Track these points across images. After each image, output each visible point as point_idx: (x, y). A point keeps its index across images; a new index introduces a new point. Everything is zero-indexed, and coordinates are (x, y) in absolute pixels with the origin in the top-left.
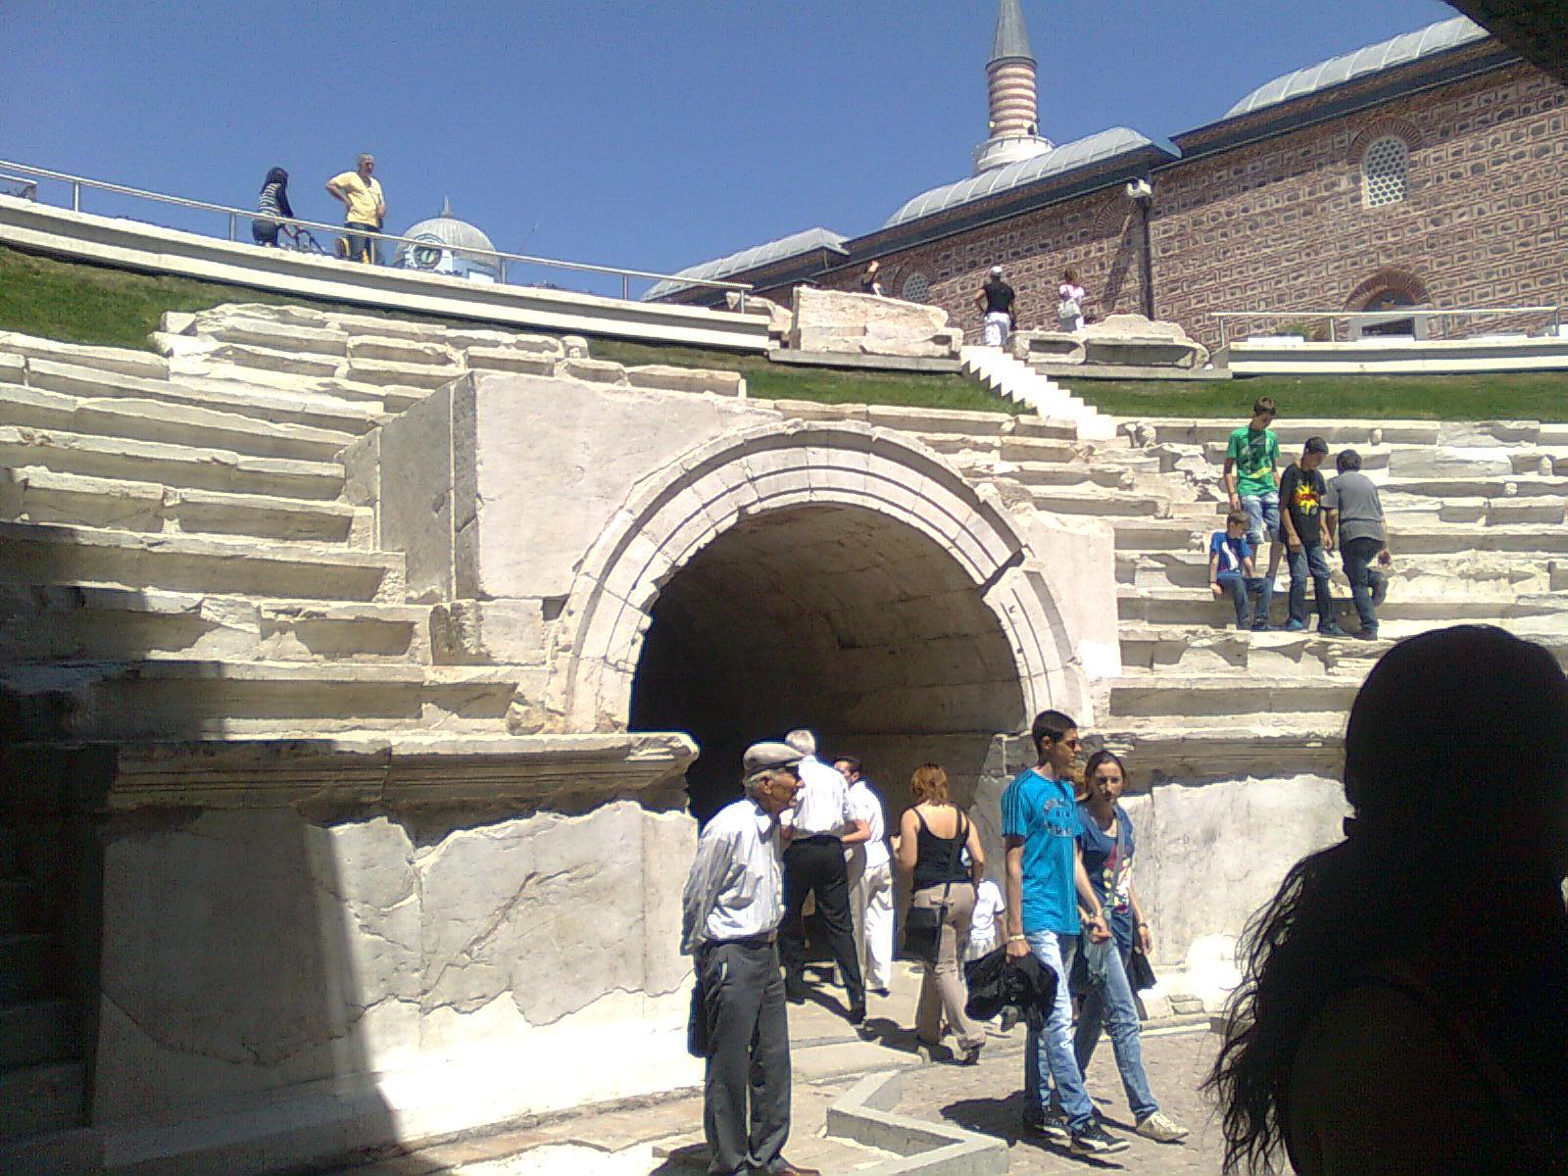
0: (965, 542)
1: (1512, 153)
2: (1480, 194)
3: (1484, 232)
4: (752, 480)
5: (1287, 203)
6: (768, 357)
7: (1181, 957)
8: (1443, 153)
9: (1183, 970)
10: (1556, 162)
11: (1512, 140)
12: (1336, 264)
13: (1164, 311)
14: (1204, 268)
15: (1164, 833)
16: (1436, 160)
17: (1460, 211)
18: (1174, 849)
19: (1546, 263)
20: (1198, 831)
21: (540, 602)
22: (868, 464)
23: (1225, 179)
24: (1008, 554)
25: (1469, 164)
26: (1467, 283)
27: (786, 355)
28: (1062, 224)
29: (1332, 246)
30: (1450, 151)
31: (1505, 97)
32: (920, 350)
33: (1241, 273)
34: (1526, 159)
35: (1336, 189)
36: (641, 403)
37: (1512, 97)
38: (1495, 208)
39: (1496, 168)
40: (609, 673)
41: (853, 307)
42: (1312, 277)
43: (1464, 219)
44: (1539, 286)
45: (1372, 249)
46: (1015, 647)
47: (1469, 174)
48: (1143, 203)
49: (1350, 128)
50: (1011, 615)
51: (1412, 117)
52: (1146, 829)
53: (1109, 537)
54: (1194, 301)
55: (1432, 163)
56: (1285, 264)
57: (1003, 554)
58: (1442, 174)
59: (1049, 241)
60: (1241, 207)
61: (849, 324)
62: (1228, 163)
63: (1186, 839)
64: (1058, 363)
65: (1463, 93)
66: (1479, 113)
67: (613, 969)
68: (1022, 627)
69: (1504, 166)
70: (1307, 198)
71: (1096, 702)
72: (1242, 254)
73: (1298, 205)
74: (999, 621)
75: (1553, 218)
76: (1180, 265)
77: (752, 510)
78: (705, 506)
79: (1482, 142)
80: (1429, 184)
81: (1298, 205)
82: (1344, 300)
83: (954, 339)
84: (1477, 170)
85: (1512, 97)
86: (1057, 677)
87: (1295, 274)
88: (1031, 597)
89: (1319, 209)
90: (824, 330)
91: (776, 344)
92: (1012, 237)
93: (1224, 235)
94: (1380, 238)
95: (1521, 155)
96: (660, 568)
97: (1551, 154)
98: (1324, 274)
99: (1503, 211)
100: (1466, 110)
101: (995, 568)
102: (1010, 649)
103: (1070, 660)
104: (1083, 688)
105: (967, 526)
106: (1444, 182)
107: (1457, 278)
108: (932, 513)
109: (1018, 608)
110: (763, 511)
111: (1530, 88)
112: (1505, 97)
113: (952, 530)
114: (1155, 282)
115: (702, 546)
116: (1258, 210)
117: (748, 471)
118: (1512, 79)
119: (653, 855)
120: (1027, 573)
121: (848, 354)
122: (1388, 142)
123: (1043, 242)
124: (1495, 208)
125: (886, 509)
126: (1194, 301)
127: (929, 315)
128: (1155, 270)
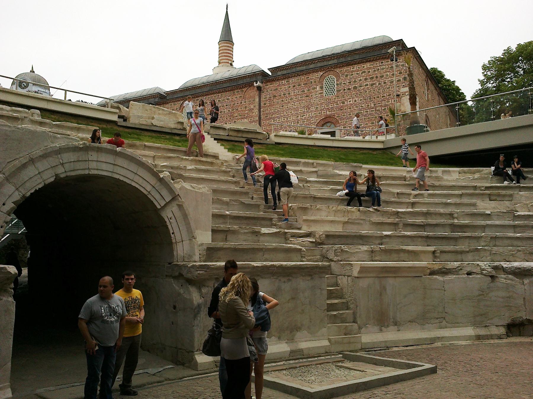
0: (154, 193)
1: (365, 84)
2: (356, 95)
3: (356, 107)
4: (62, 164)
5: (301, 93)
6: (117, 123)
8: (346, 82)
10: (376, 88)
11: (365, 80)
12: (314, 113)
13: (264, 123)
14: (276, 111)
16: (345, 83)
17: (350, 100)
19: (372, 118)
22: (115, 161)
23: (284, 83)
24: (170, 198)
25: (353, 86)
26: (350, 122)
27: (124, 124)
28: (234, 93)
29: (314, 107)
30: (348, 82)
31: (363, 67)
32: (173, 126)
33: (287, 113)
34: (369, 86)
35: (316, 90)
36: (13, 131)
37: (365, 67)
38: (359, 101)
39: (360, 88)
41: (150, 110)
42: (308, 116)
43: (351, 102)
44: (370, 124)
45: (325, 109)
46: (171, 232)
47: (353, 89)
48: (259, 88)
49: (321, 71)
50: (170, 220)
51: (338, 70)
53: (210, 193)
54: (272, 121)
55: (343, 85)
56: (299, 111)
57: (168, 198)
58: (345, 88)
59: (230, 98)
60: (288, 93)
61: (149, 115)
62: (285, 79)
65: (352, 65)
66: (356, 71)
68: (174, 224)
69: (363, 87)
70: (307, 92)
71: (201, 252)
72: (288, 107)
73: (305, 94)
74: (166, 222)
75: (375, 104)
76: (269, 109)
77: (62, 176)
79: (357, 80)
80: (341, 91)
81: (305, 94)
82: (316, 124)
84: (355, 88)
85: (365, 67)
86: (186, 243)
87: (302, 115)
88: (178, 213)
89: (310, 95)
90: (139, 117)
91: (122, 120)
92: (218, 96)
93: (282, 101)
94: (327, 106)
95: (367, 85)
96: (17, 197)
97: (375, 86)
98: (311, 116)
99: (362, 101)
100: (353, 70)
101: (166, 203)
102: (170, 232)
103: (192, 237)
104: (196, 247)
105: (155, 187)
106: (346, 91)
107: (348, 120)
108: (141, 181)
109: (173, 217)
110: (67, 176)
111: (370, 65)
112: (363, 67)
113: (149, 188)
114: (262, 113)
115: (37, 189)
116: (293, 94)
117: (61, 161)
118: (366, 62)
120: (178, 205)
121: (147, 125)
122: (331, 77)
123: (228, 98)
124: (359, 101)
125: (122, 178)
126: (272, 121)
127: (178, 115)
128: (262, 110)
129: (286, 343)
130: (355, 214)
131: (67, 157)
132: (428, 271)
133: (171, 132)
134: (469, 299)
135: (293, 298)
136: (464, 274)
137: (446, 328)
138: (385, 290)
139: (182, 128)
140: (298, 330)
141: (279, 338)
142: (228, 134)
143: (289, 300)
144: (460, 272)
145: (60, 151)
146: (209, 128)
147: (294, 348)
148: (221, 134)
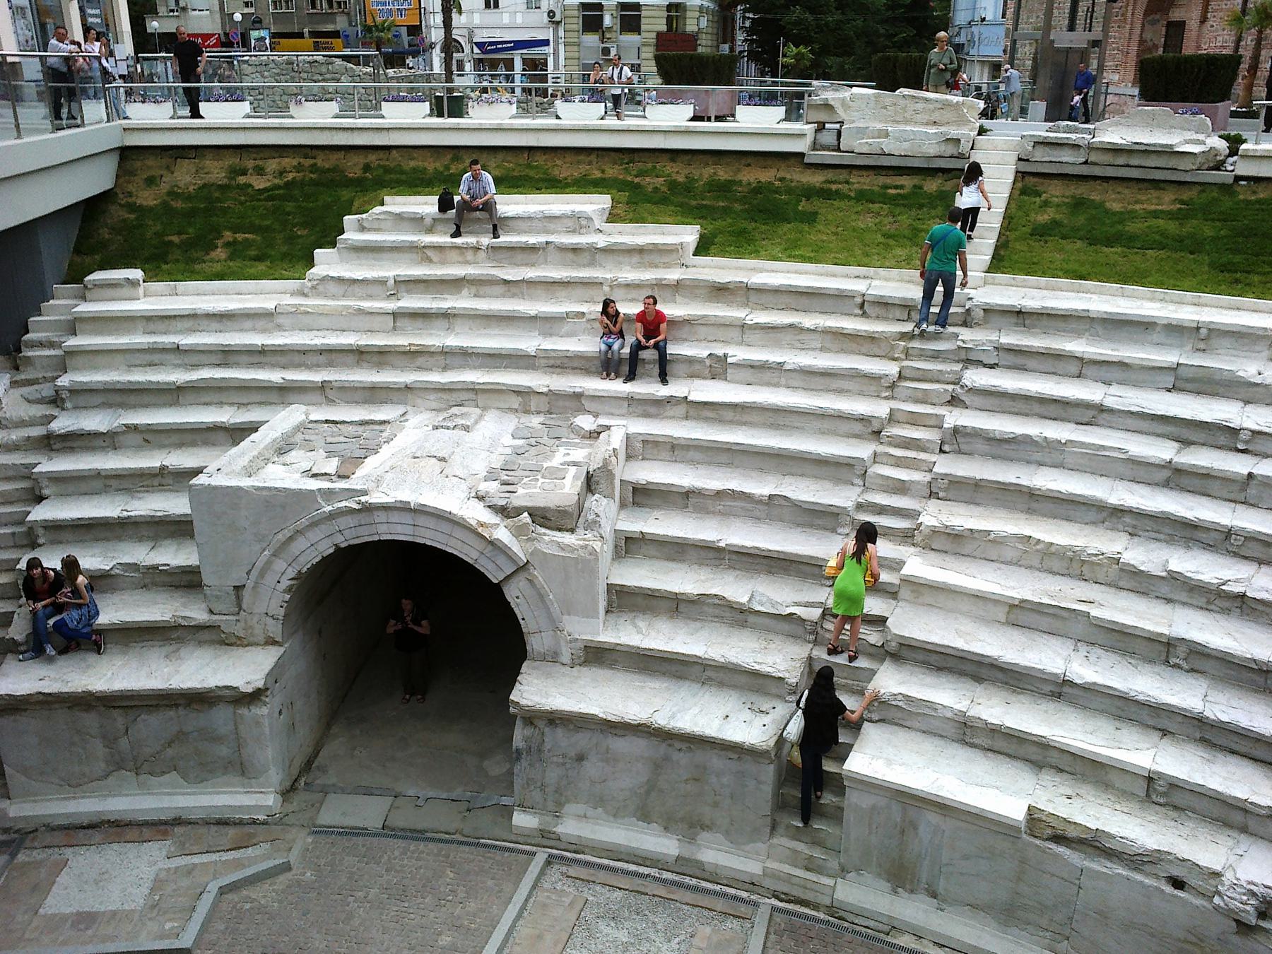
9: (557, 816)
20: (573, 754)
32: (932, 150)
40: (269, 620)
46: (520, 617)
52: (538, 746)
63: (564, 756)
64: (1059, 162)
67: (226, 768)
77: (343, 545)
83: (962, 142)
88: (528, 591)
96: (291, 573)
103: (557, 629)
119: (241, 727)
129: (679, 840)
130: (1105, 569)
131: (344, 522)
132: (1049, 831)
133: (926, 166)
134: (1152, 935)
136: (1157, 877)
138: (915, 828)
139: (956, 154)
140: (706, 829)
142: (1084, 160)
144: (1147, 868)
145: (332, 516)
146: (1030, 148)
147: (686, 855)
148: (1065, 159)
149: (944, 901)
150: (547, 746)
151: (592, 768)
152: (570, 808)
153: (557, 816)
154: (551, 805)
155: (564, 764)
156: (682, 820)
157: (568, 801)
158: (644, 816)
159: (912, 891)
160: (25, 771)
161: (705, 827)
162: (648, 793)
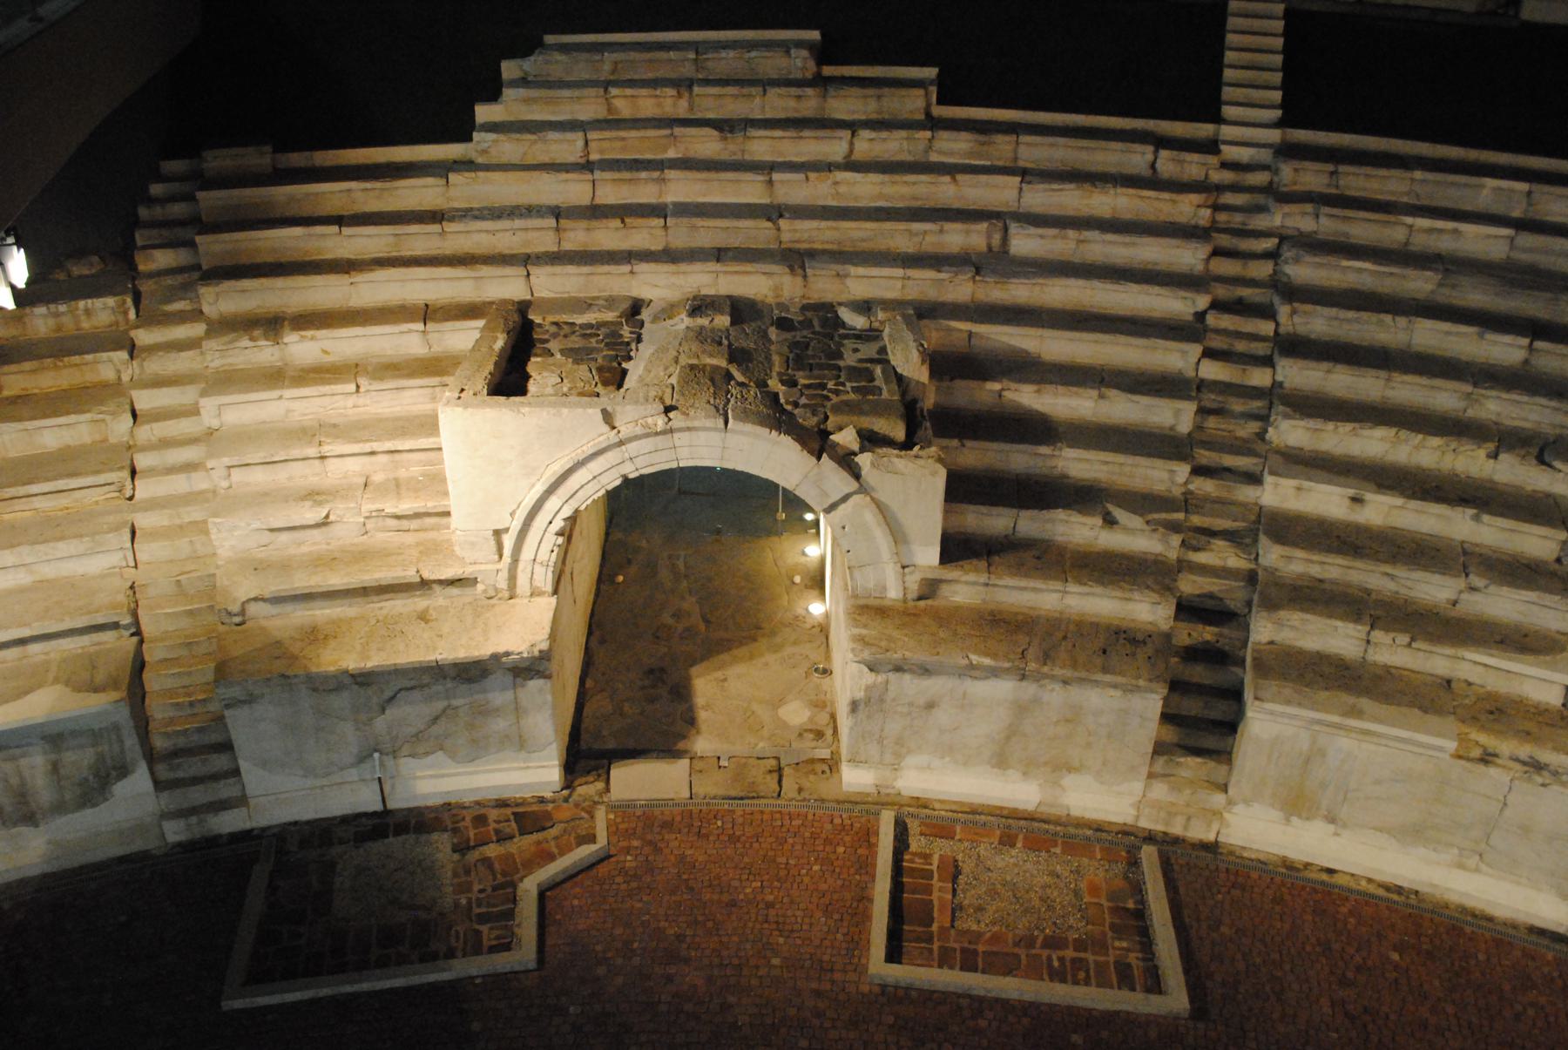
7: (896, 762)
9: (896, 769)
15: (894, 700)
18: (899, 709)
21: (492, 532)
77: (631, 476)
78: (595, 477)
129: (1040, 785)
135: (1067, 721)
137: (1477, 870)
141: (1025, 774)
143: (1058, 721)
149: (1345, 826)
150: (891, 694)
151: (942, 716)
152: (910, 761)
153: (896, 769)
154: (888, 758)
155: (910, 713)
156: (1046, 764)
157: (909, 752)
158: (1001, 761)
159: (1308, 819)
160: (264, 764)
161: (1070, 769)
162: (1008, 738)
